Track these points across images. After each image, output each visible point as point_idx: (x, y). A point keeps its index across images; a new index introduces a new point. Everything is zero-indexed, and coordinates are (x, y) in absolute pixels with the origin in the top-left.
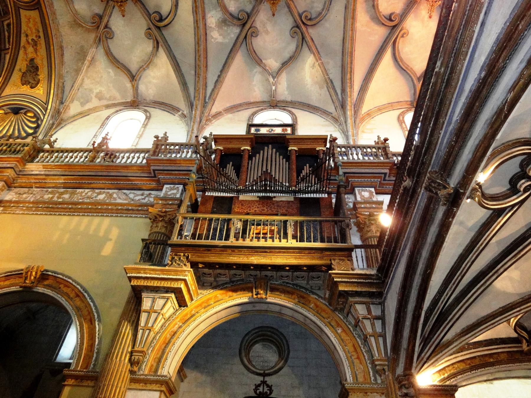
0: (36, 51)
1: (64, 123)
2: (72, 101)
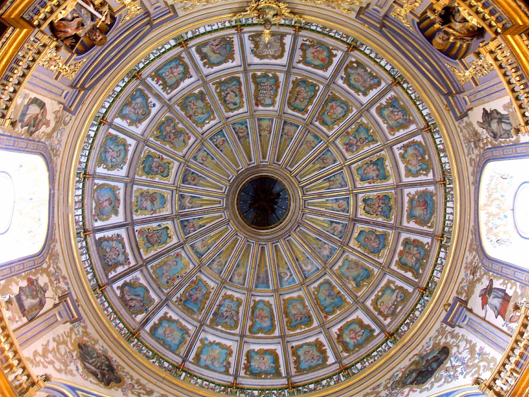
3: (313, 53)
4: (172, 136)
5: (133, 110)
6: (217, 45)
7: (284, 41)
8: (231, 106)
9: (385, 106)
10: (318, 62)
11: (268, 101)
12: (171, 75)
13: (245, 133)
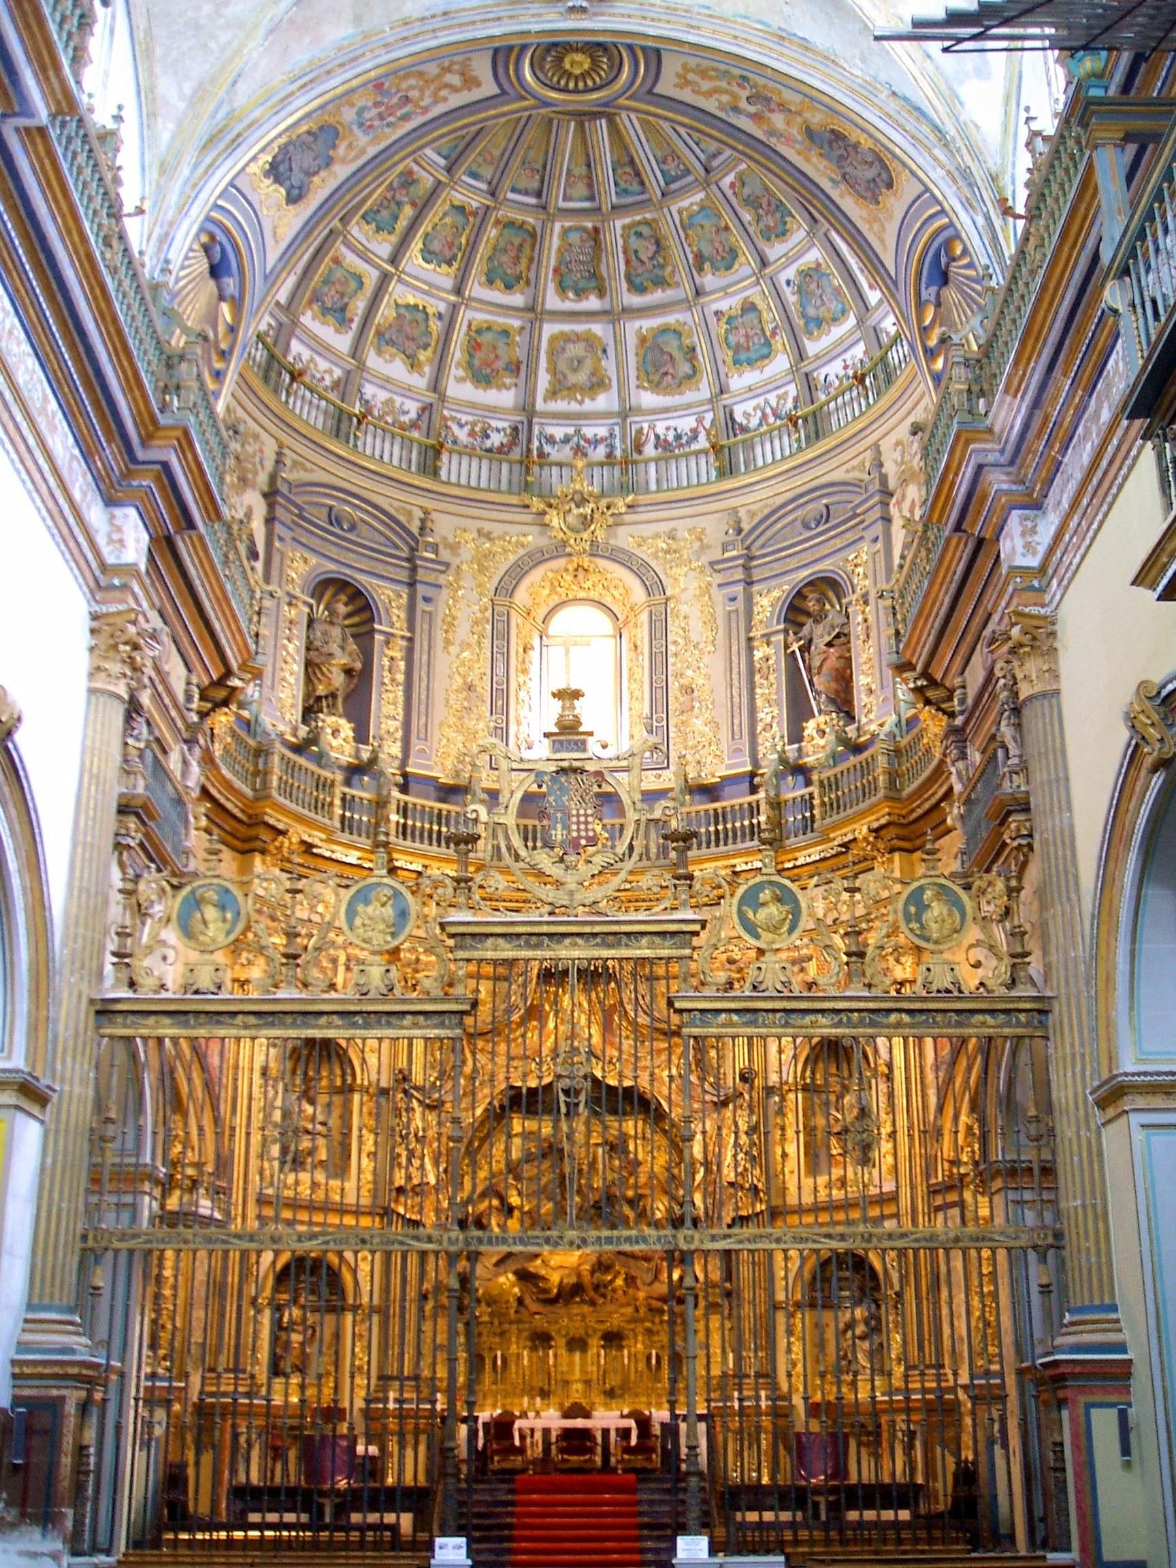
0: (783, 107)
1: (1008, 179)
2: (953, 99)
4: (764, 202)
7: (548, 377)
8: (645, 230)
10: (487, 338)
11: (574, 238)
12: (751, 333)
13: (619, 171)
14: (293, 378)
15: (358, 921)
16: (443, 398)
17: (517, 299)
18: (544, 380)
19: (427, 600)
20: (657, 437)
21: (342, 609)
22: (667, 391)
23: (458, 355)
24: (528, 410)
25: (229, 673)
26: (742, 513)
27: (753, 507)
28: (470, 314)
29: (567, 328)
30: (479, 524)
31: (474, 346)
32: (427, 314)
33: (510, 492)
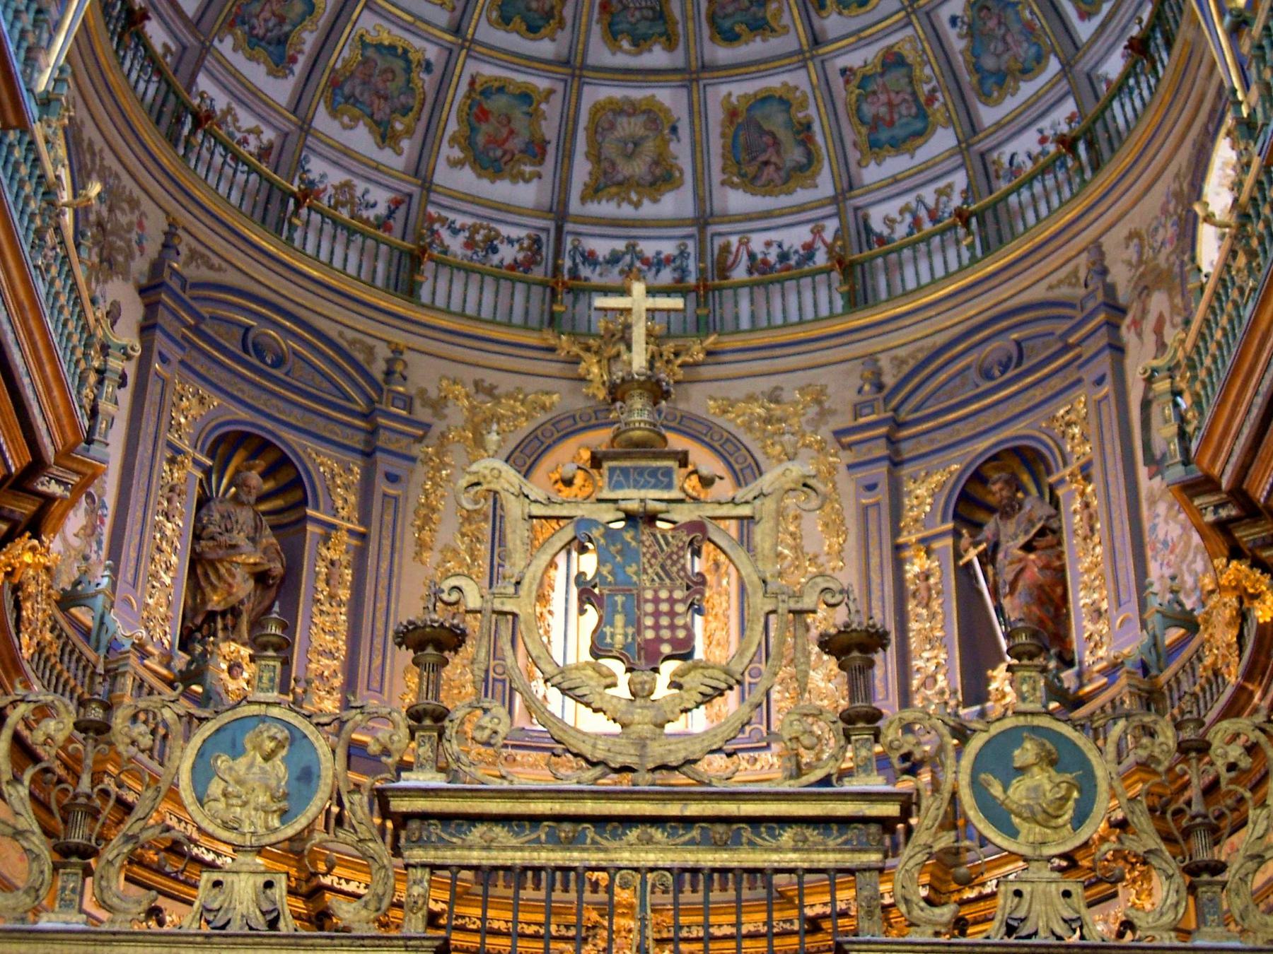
3: (512, 132)
5: (1009, 39)
6: (766, 163)
9: (304, 29)
10: (498, 103)
12: (896, 100)
14: (197, 123)
15: (215, 788)
16: (427, 186)
17: (545, 48)
18: (581, 170)
19: (392, 478)
20: (752, 256)
21: (254, 478)
22: (769, 189)
23: (453, 127)
24: (559, 213)
25: (37, 466)
26: (884, 362)
27: (902, 353)
28: (473, 67)
29: (618, 93)
30: (479, 374)
31: (476, 113)
32: (408, 62)
33: (525, 327)
